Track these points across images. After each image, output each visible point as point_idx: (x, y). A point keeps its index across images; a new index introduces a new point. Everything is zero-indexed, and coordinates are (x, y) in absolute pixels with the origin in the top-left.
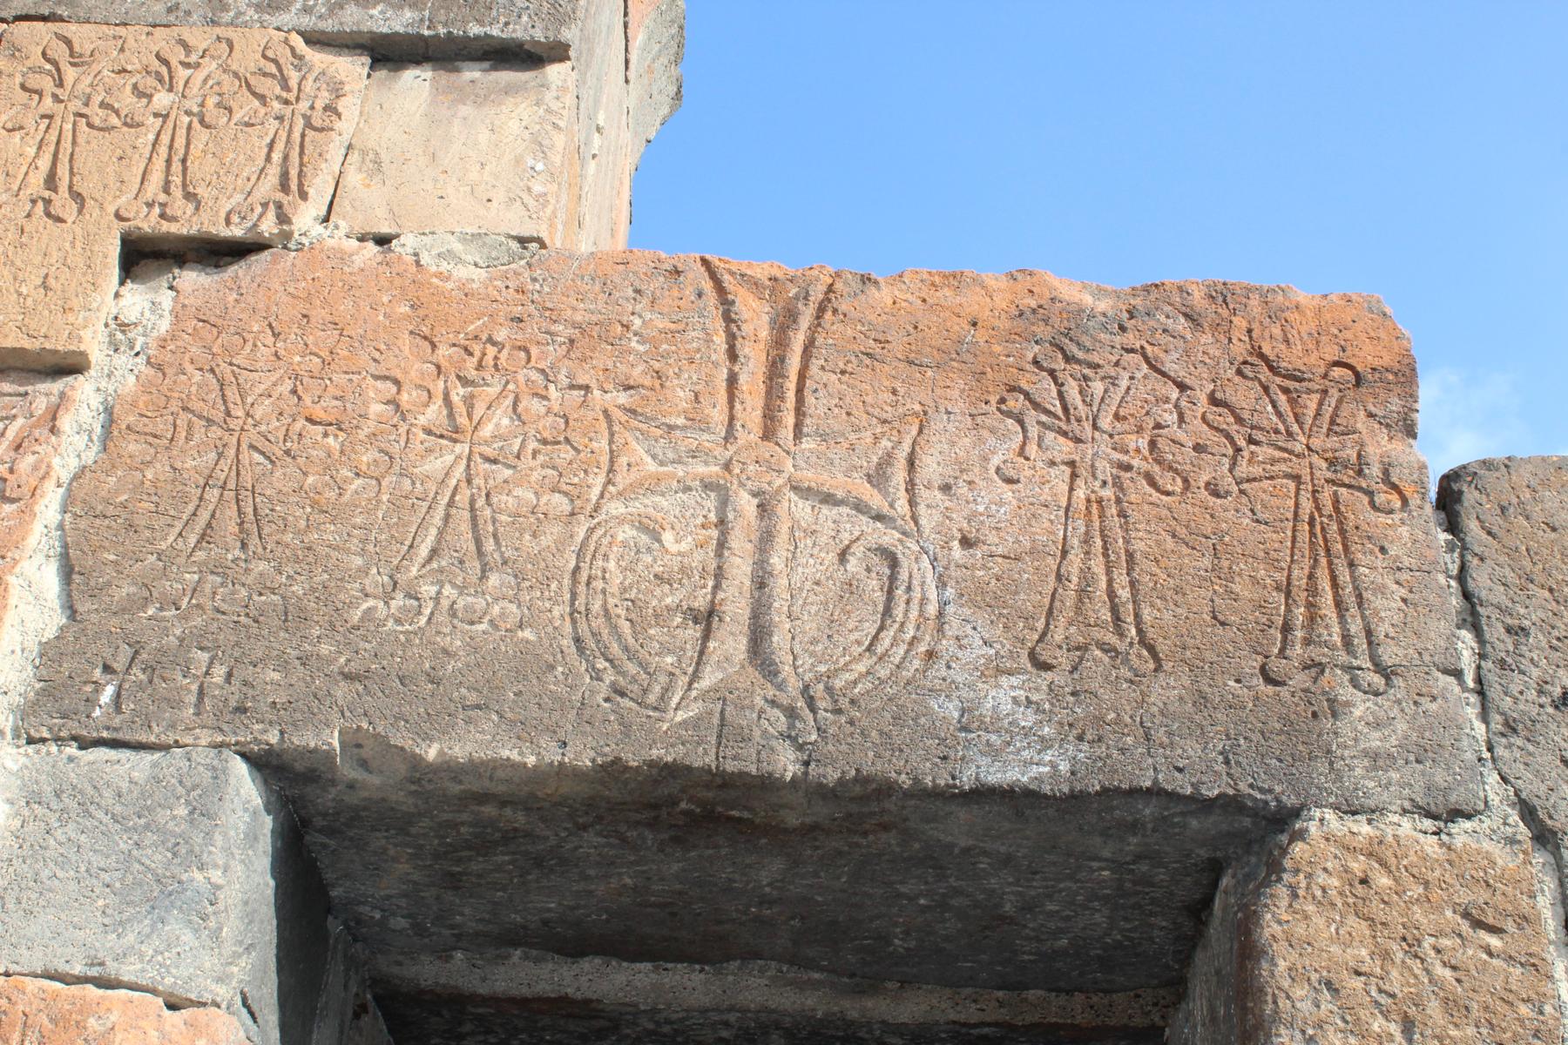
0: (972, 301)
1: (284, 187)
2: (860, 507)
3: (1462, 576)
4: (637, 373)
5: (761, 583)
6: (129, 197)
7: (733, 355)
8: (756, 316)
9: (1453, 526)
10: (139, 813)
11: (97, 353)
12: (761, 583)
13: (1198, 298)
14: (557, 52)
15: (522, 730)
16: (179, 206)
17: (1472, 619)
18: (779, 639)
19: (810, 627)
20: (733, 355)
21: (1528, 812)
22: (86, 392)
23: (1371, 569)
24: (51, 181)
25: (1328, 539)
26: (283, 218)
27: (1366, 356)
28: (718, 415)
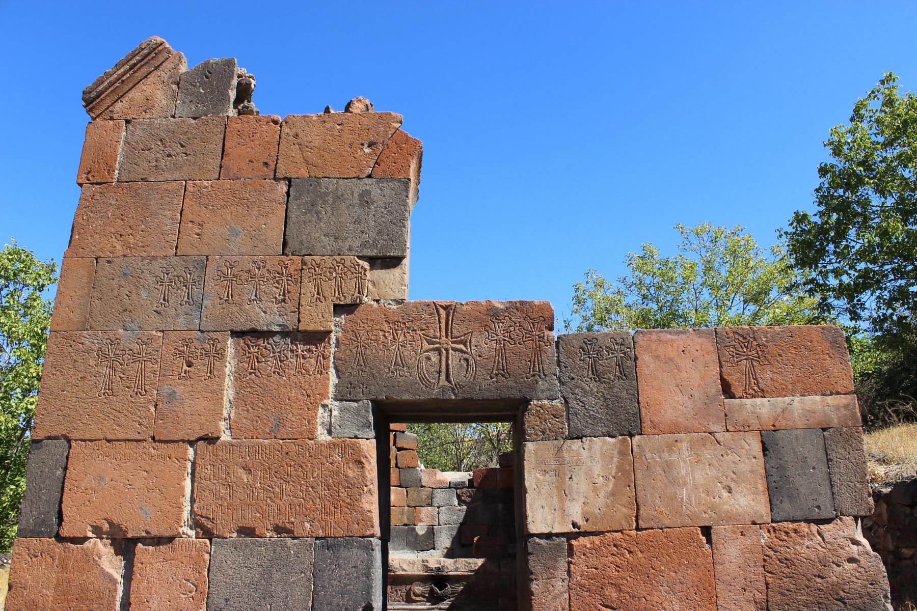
0: (480, 308)
1: (359, 293)
2: (462, 351)
3: (558, 357)
4: (424, 327)
5: (447, 365)
6: (332, 297)
7: (440, 322)
8: (443, 313)
9: (557, 347)
10: (357, 412)
11: (333, 328)
12: (447, 365)
13: (518, 305)
14: (404, 257)
15: (413, 394)
16: (342, 298)
17: (559, 365)
18: (451, 377)
19: (456, 373)
20: (440, 322)
21: (564, 398)
22: (333, 336)
23: (544, 357)
24: (318, 294)
25: (539, 351)
26: (360, 300)
27: (546, 314)
28: (438, 334)
